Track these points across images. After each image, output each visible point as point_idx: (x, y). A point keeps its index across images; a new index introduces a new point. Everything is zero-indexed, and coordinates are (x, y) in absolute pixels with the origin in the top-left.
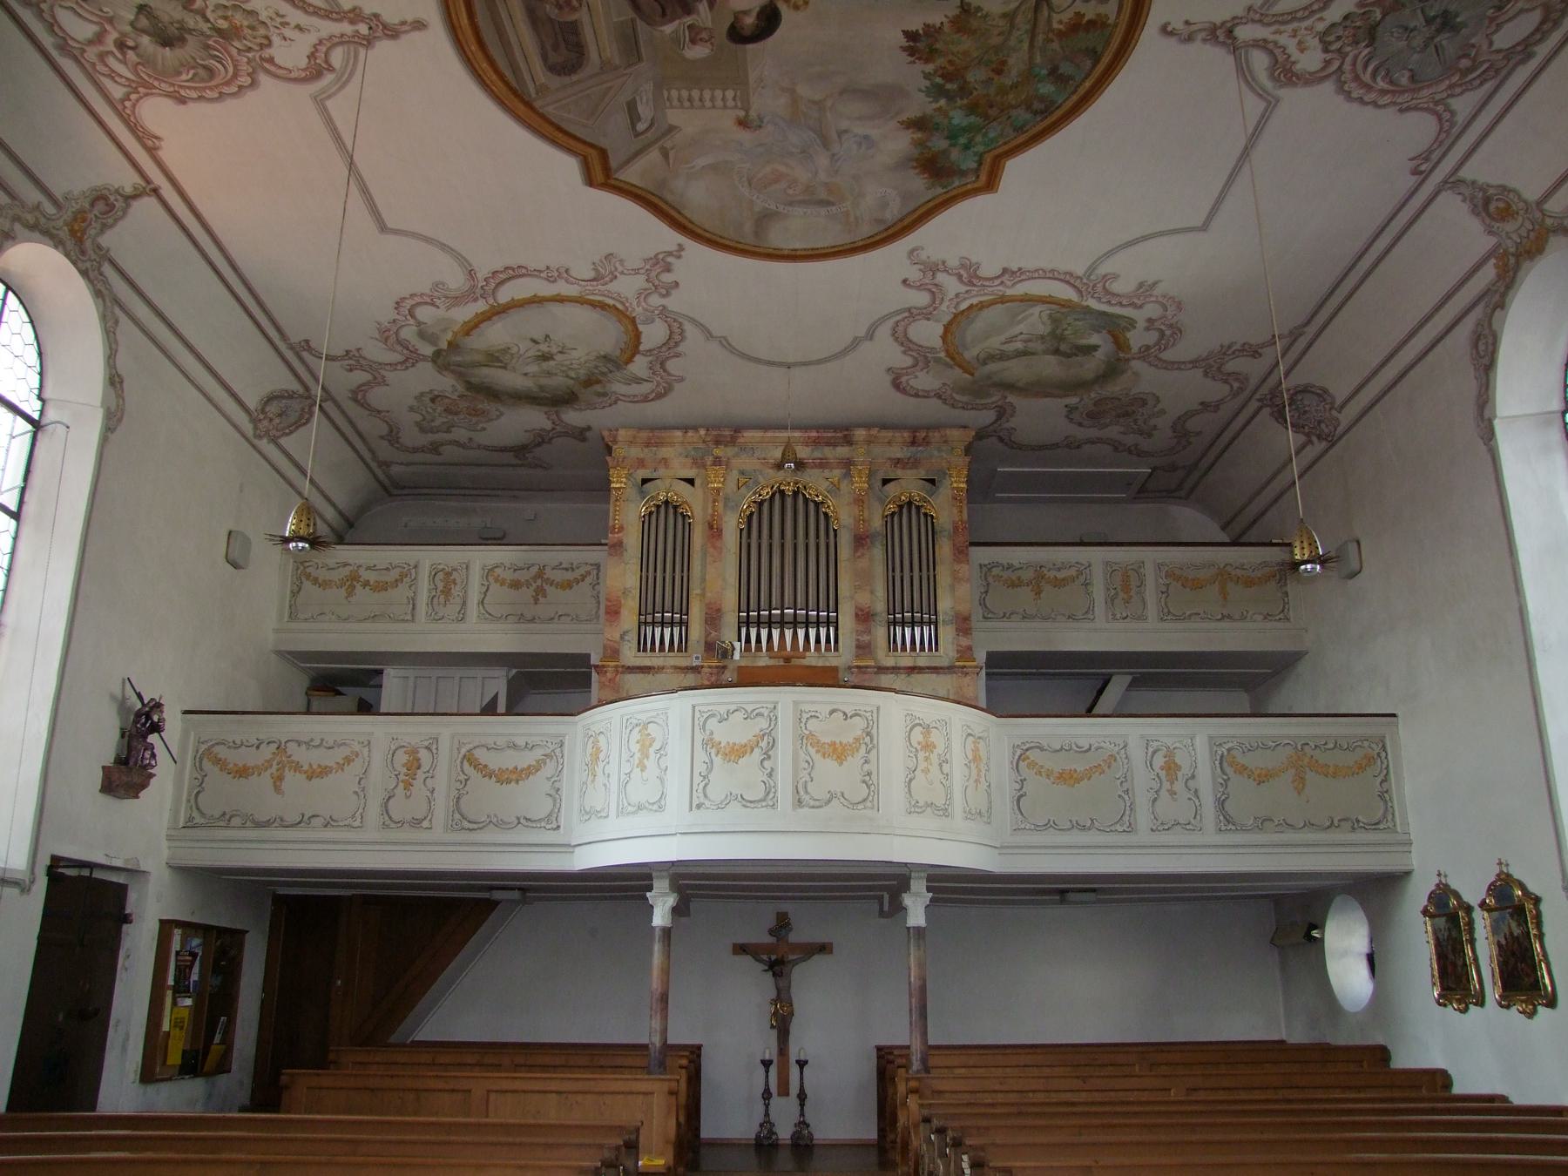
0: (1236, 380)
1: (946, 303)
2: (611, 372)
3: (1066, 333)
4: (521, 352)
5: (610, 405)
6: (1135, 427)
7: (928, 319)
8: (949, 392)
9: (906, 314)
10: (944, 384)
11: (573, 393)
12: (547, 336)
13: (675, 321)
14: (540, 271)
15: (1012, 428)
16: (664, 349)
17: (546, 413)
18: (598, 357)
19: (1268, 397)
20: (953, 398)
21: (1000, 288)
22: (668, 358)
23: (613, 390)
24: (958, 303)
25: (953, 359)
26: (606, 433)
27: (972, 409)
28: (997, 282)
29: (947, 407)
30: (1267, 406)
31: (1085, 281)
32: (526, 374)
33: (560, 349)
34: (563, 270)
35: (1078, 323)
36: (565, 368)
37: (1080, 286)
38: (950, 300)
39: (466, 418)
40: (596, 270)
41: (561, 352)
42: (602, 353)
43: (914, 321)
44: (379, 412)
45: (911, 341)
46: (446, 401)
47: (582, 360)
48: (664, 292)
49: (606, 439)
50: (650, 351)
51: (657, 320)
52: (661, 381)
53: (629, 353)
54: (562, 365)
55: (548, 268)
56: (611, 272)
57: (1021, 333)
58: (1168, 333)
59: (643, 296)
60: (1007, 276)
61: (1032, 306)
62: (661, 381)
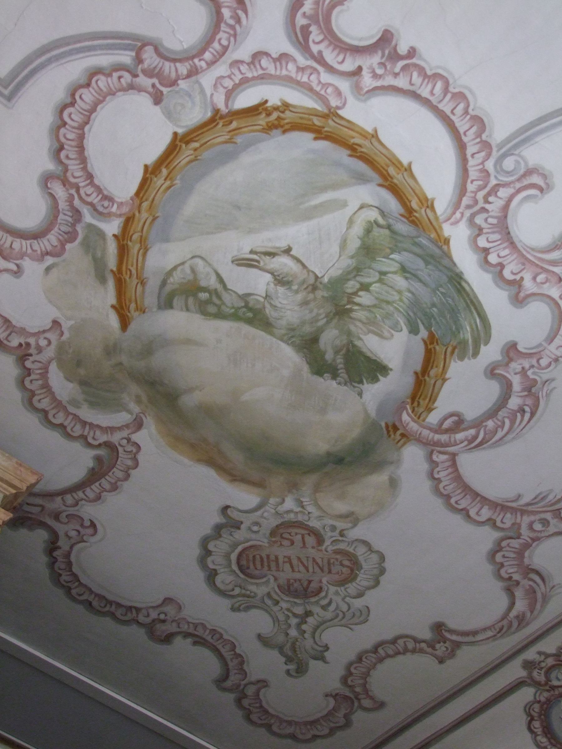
0: (531, 593)
1: (221, 69)
3: (364, 298)
6: (293, 633)
7: (158, 99)
8: (50, 352)
9: (126, 58)
10: (56, 323)
15: (93, 525)
19: (550, 661)
20: (44, 374)
21: (344, 85)
24: (245, 82)
25: (123, 250)
27: (62, 427)
28: (349, 65)
29: (17, 395)
30: (537, 684)
31: (490, 165)
35: (400, 282)
37: (473, 174)
38: (237, 63)
43: (131, 87)
45: (81, 148)
57: (288, 251)
58: (514, 402)
60: (376, 59)
61: (361, 179)
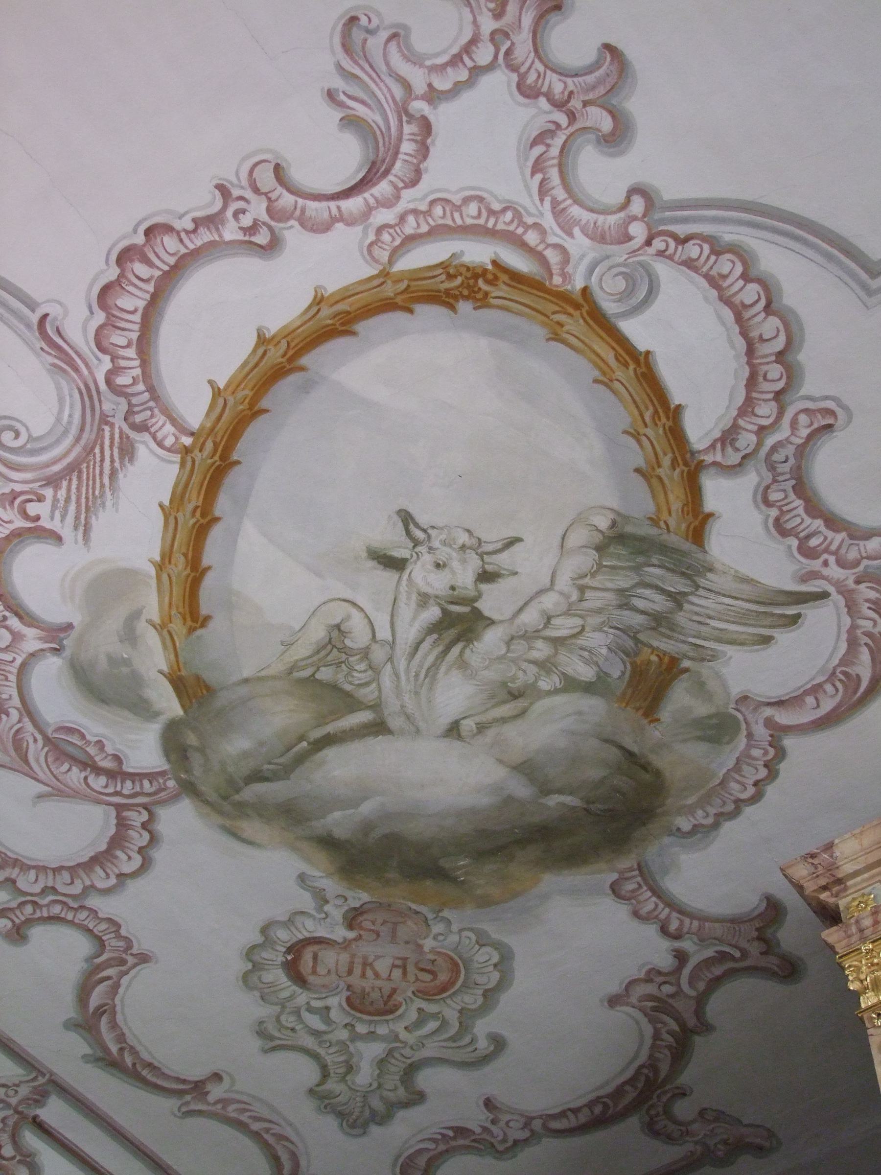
2: (678, 599)
4: (383, 633)
5: (772, 774)
11: (629, 754)
12: (406, 518)
13: (718, 249)
14: (212, 221)
16: (766, 410)
17: (615, 889)
18: (600, 549)
22: (802, 451)
23: (735, 691)
26: (801, 872)
32: (453, 730)
33: (474, 563)
34: (266, 178)
36: (542, 650)
39: (423, 1017)
40: (351, 122)
41: (486, 577)
42: (603, 522)
44: (198, 1088)
46: (330, 958)
47: (564, 582)
48: (606, 124)
49: (810, 887)
50: (728, 438)
51: (663, 270)
52: (847, 576)
53: (676, 498)
54: (529, 636)
55: (223, 190)
56: (403, 111)
59: (554, 174)
62: (847, 576)
